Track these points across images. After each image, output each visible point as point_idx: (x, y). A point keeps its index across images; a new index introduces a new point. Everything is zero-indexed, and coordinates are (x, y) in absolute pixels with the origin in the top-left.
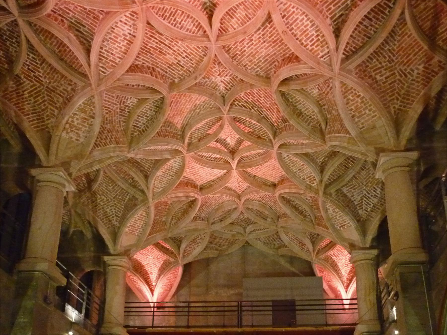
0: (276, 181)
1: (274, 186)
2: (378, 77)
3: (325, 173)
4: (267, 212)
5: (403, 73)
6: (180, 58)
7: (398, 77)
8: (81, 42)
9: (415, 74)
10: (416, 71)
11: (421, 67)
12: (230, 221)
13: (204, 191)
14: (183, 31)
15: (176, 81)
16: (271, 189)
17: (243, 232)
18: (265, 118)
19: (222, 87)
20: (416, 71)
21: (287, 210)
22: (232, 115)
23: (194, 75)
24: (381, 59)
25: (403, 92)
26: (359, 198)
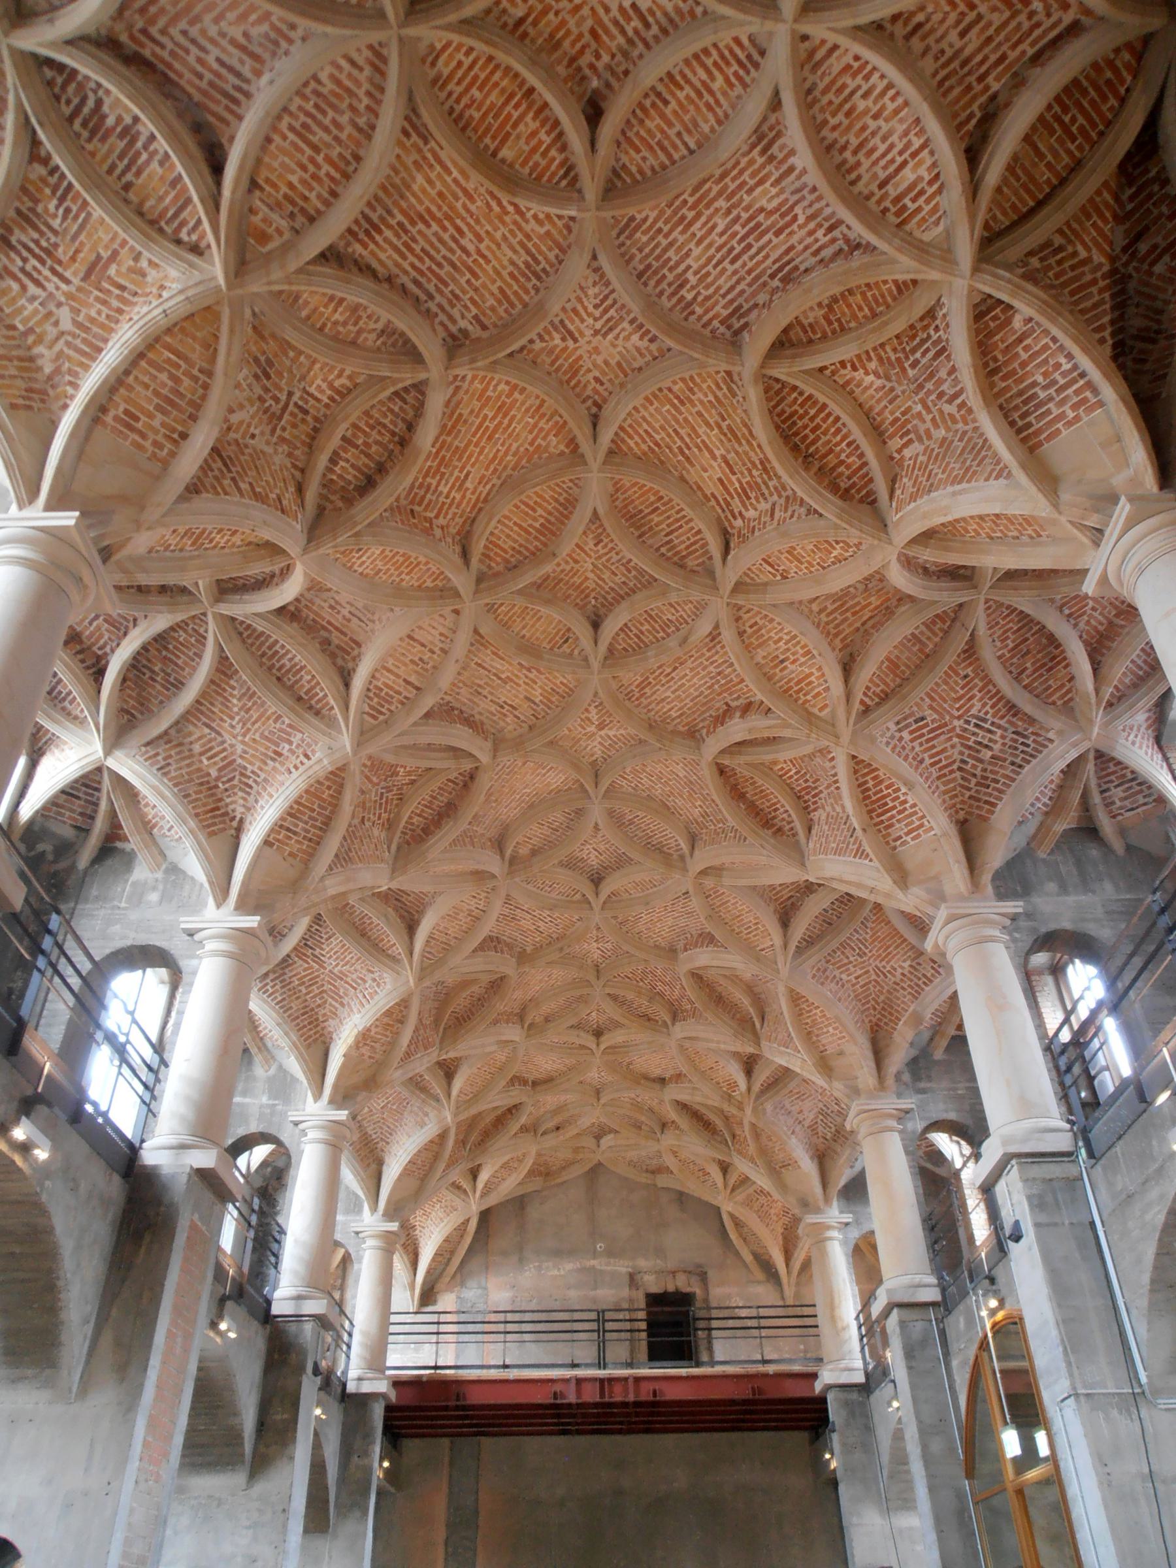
0: (667, 1076)
1: (662, 1081)
2: (844, 976)
3: (754, 1076)
4: (643, 1119)
5: (879, 971)
6: (541, 924)
7: (874, 977)
8: (401, 917)
9: (898, 974)
10: (900, 971)
11: (906, 965)
12: (575, 1132)
13: (538, 1088)
14: (553, 895)
15: (529, 949)
16: (657, 1086)
17: (594, 1147)
18: (661, 995)
19: (596, 955)
20: (900, 971)
21: (683, 1122)
22: (608, 990)
23: (559, 945)
24: (848, 951)
25: (882, 998)
26: (812, 1116)
